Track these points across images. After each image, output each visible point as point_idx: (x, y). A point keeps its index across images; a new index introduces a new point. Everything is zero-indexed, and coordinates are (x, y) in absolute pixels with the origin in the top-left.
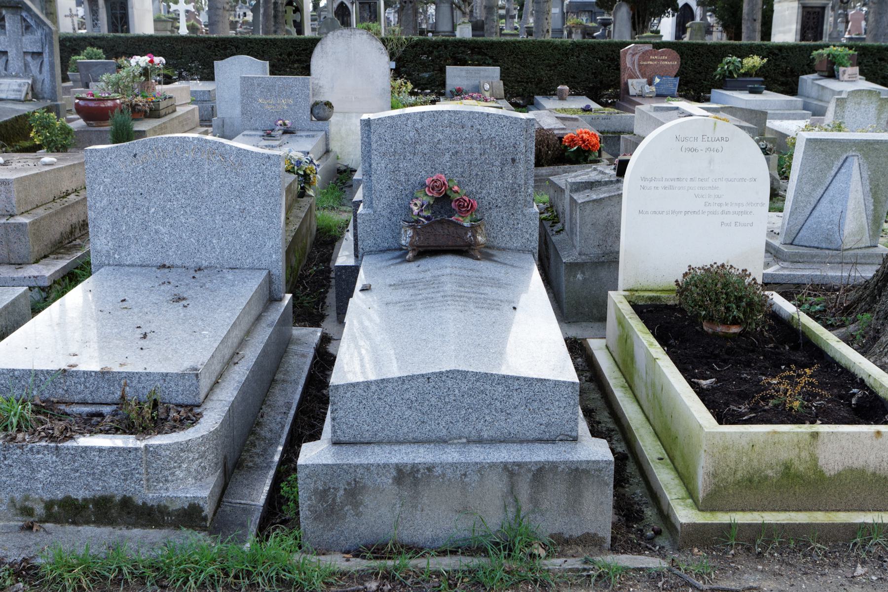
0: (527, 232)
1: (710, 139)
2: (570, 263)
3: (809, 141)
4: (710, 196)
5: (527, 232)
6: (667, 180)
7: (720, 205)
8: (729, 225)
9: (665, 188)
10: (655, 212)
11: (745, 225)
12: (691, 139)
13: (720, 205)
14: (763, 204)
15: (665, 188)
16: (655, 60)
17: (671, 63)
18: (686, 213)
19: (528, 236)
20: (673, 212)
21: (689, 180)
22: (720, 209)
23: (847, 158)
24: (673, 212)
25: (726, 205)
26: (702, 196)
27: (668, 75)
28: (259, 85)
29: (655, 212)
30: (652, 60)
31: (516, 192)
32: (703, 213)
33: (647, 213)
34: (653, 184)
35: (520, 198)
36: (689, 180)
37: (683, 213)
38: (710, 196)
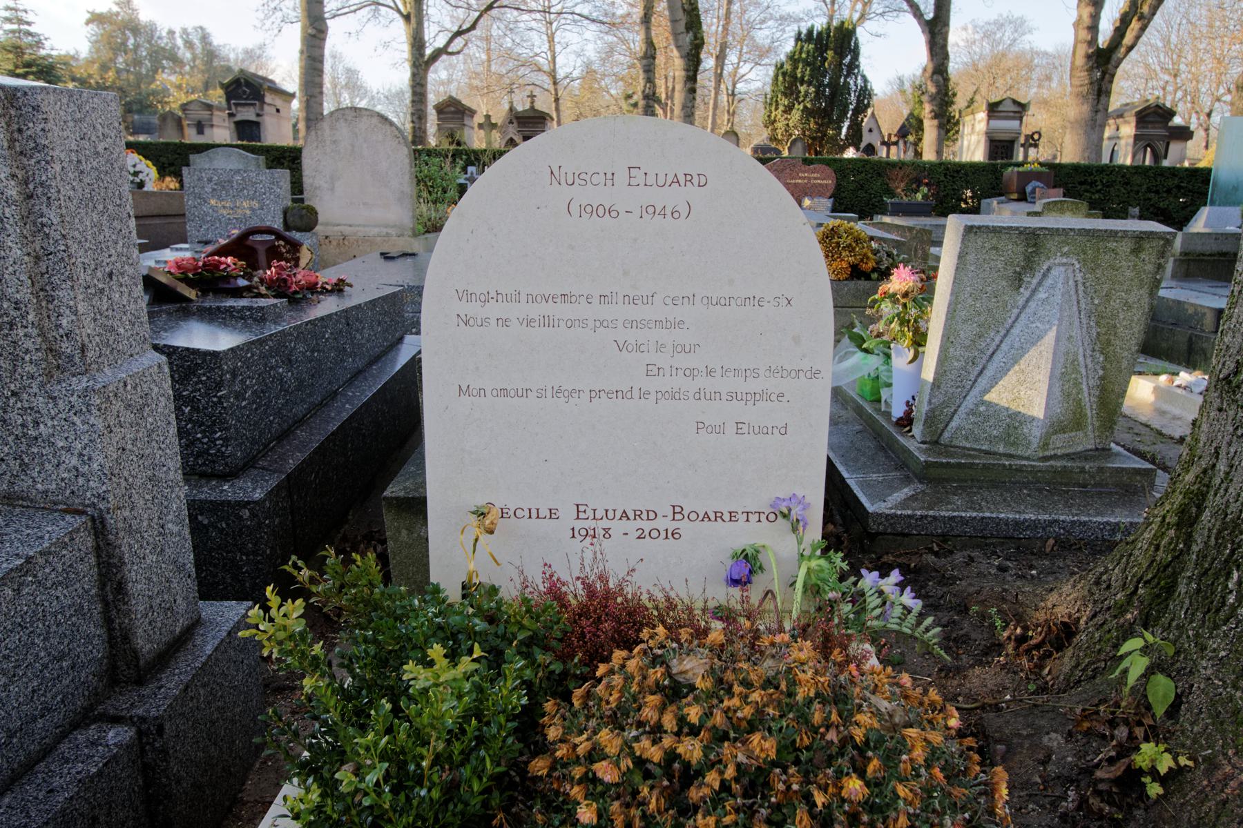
0: (69, 449)
1: (651, 180)
2: (397, 498)
3: (969, 230)
4: (659, 347)
5: (69, 449)
6: (531, 298)
7: (691, 373)
8: (719, 430)
9: (529, 323)
10: (504, 392)
11: (763, 431)
12: (595, 179)
13: (691, 373)
14: (815, 374)
15: (529, 323)
16: (804, 178)
17: (825, 182)
18: (595, 394)
19: (74, 461)
20: (557, 392)
21: (596, 300)
22: (690, 386)
23: (1049, 269)
24: (557, 392)
25: (710, 373)
26: (638, 348)
27: (821, 195)
28: (210, 180)
29: (504, 392)
30: (800, 178)
31: (12, 325)
32: (644, 395)
33: (482, 392)
34: (494, 310)
35: (29, 344)
36: (596, 300)
37: (585, 396)
38: (659, 347)
